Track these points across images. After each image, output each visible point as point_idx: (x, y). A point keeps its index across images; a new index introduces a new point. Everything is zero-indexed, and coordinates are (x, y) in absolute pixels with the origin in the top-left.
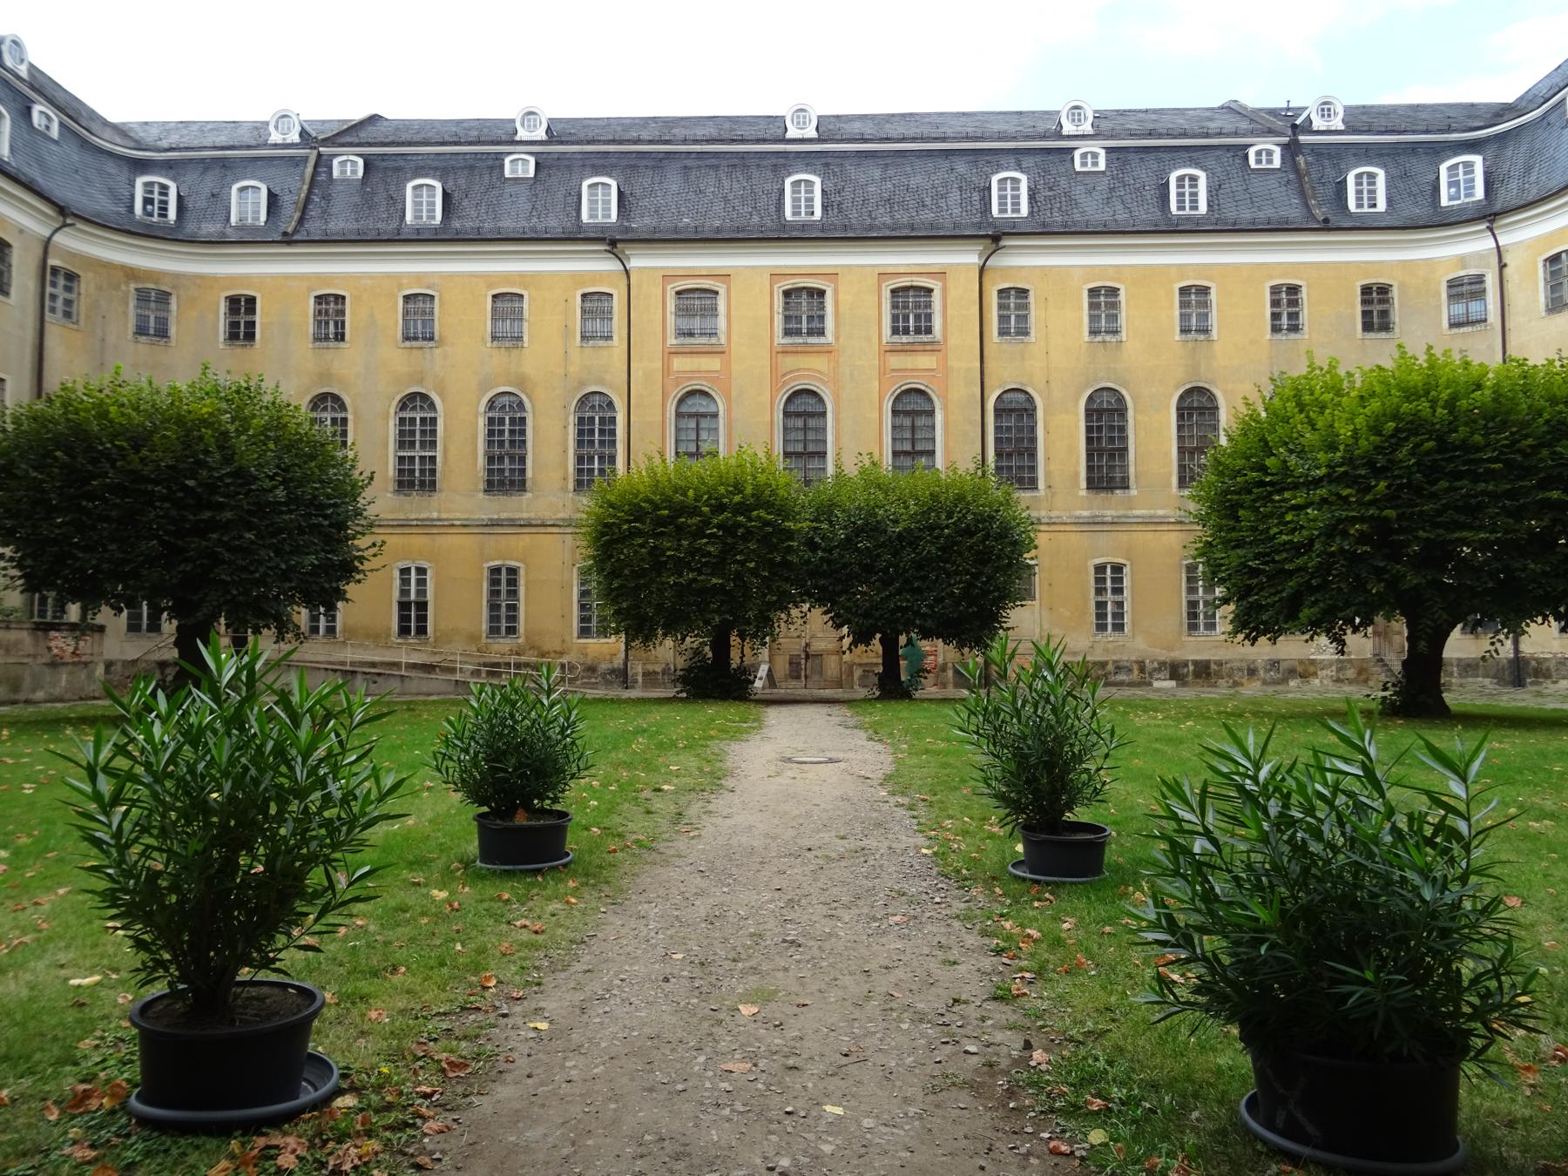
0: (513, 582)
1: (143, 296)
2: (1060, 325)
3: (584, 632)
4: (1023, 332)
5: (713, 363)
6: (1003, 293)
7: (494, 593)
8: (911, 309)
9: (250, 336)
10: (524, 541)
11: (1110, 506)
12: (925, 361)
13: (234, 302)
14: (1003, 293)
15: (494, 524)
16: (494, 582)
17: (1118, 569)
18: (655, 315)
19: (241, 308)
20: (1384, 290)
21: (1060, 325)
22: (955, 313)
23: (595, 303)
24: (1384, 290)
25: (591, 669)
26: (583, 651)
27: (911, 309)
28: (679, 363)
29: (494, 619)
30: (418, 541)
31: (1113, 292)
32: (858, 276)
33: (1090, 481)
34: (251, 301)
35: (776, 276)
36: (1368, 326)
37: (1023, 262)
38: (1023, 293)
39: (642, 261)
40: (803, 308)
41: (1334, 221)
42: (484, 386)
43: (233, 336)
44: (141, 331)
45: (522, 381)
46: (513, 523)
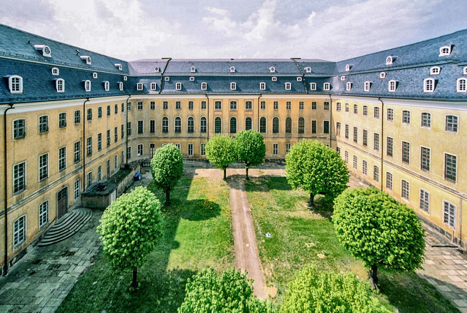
0: (192, 146)
1: (139, 104)
2: (270, 107)
3: (202, 154)
4: (264, 108)
5: (220, 113)
6: (262, 102)
7: (189, 148)
8: (249, 105)
9: (154, 108)
10: (193, 140)
11: (276, 135)
12: (250, 113)
13: (151, 103)
14: (262, 102)
15: (189, 137)
16: (189, 146)
17: (277, 145)
18: (212, 105)
19: (153, 103)
20: (315, 103)
21: (270, 107)
22: (255, 106)
23: (203, 103)
24: (315, 103)
25: (203, 160)
26: (202, 157)
27: (249, 105)
28: (216, 113)
29: (189, 152)
30: (178, 140)
31: (277, 102)
32: (241, 99)
33: (273, 132)
34: (154, 103)
35: (229, 100)
36: (313, 108)
37: (265, 97)
38: (264, 102)
39: (210, 97)
40: (233, 105)
41: (308, 92)
42: (188, 116)
43: (151, 108)
44: (139, 108)
45: (193, 115)
46: (192, 137)
